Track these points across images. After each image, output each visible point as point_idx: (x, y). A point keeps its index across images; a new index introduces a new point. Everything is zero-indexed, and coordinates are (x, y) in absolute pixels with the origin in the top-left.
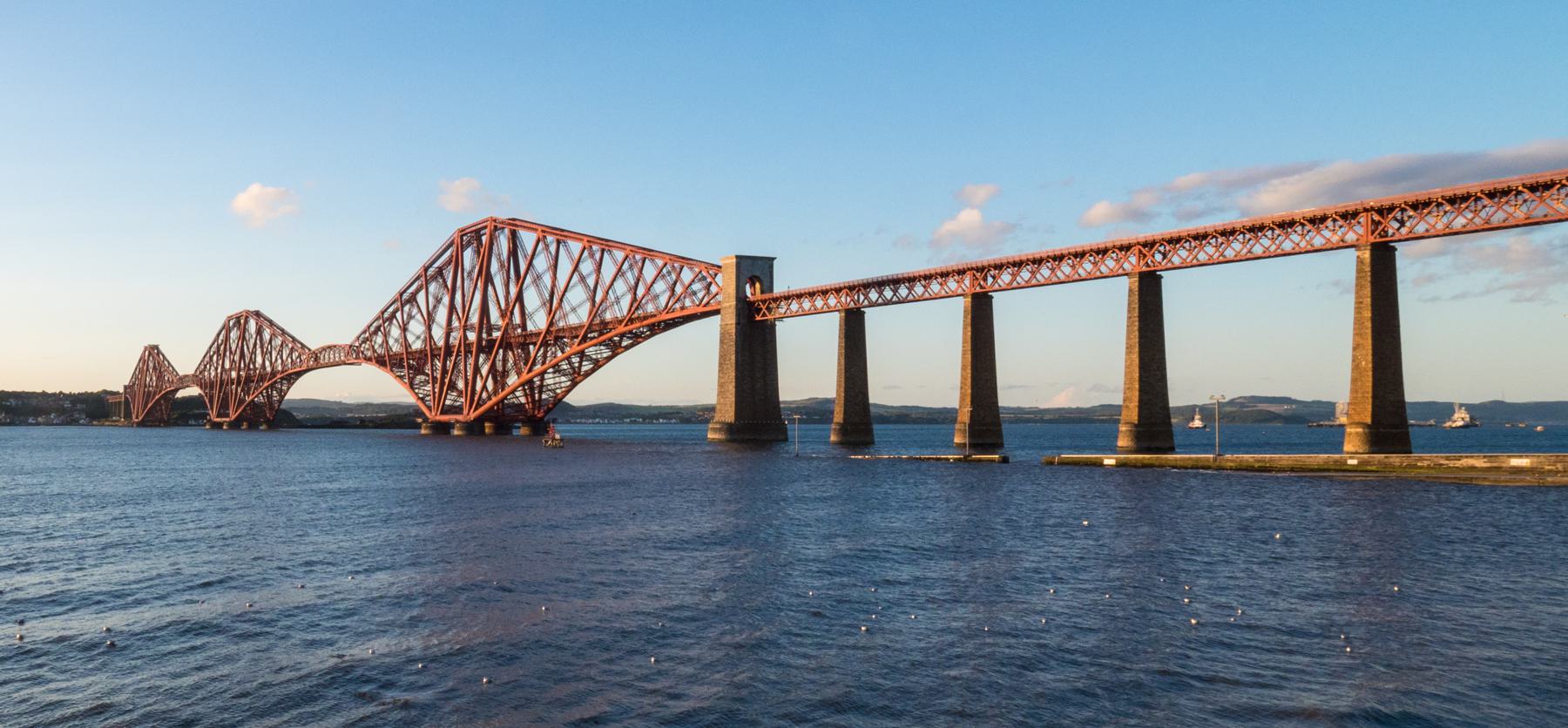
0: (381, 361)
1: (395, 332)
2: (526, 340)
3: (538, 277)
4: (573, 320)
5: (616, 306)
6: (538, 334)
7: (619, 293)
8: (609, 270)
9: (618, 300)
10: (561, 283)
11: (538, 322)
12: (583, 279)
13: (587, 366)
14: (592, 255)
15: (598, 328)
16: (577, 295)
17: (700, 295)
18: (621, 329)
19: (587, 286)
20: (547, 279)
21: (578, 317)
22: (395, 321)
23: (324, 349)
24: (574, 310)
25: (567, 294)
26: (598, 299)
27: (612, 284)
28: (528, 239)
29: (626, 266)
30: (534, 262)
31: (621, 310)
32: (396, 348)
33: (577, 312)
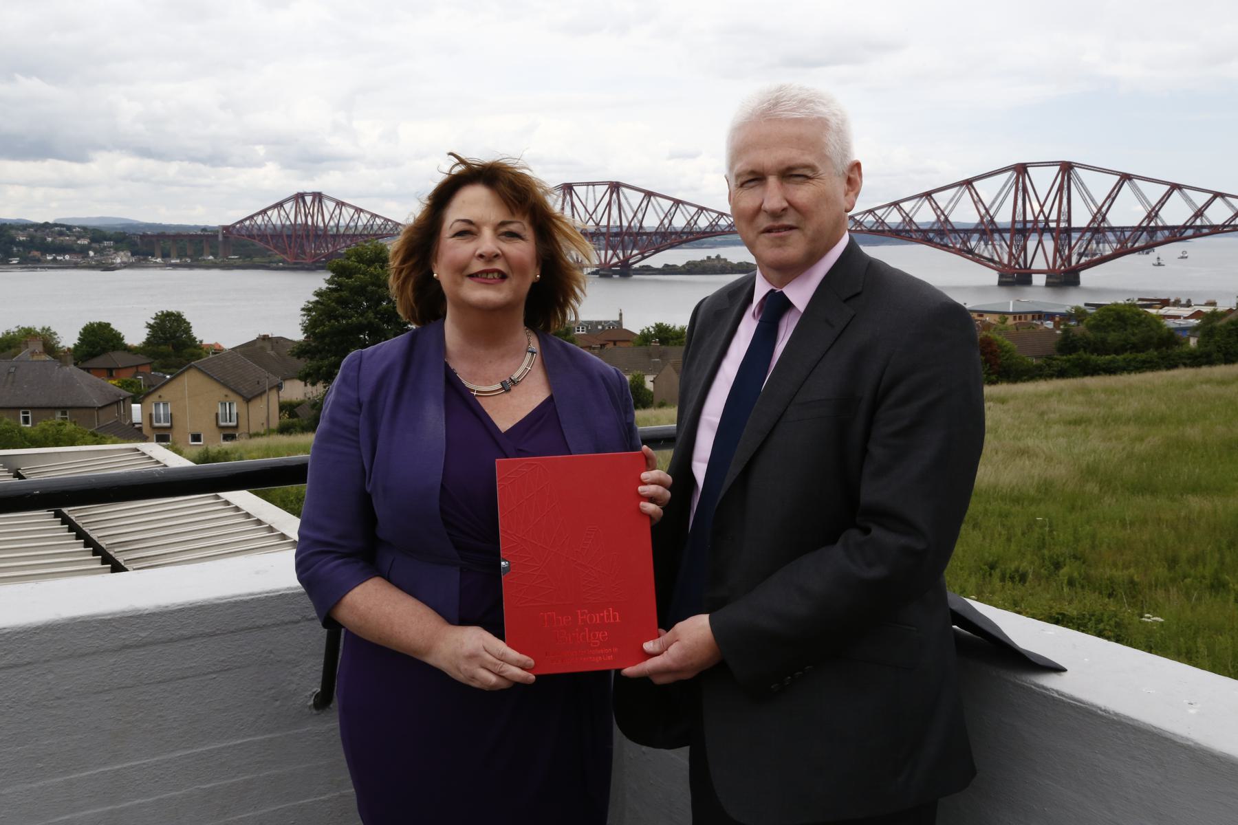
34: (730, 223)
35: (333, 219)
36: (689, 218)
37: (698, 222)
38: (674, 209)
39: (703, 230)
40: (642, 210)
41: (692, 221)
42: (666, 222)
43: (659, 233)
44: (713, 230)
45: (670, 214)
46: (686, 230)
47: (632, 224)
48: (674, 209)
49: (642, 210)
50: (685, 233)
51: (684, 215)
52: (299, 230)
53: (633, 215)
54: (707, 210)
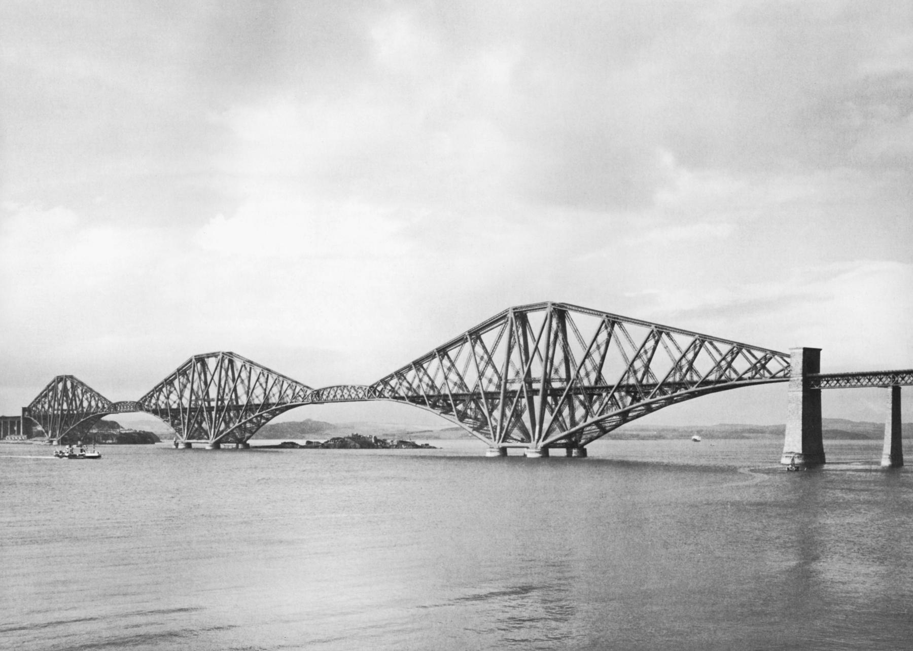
0: (155, 412)
1: (162, 398)
2: (238, 408)
3: (242, 381)
4: (256, 402)
5: (273, 398)
6: (243, 406)
7: (274, 393)
8: (271, 382)
9: (274, 395)
10: (252, 386)
11: (243, 400)
12: (261, 385)
13: (263, 421)
14: (263, 375)
15: (266, 405)
16: (259, 391)
17: (302, 396)
18: (274, 407)
19: (262, 387)
20: (246, 382)
21: (259, 400)
22: (162, 393)
23: (120, 403)
24: (257, 397)
25: (254, 391)
26: (267, 393)
27: (271, 389)
28: (238, 364)
29: (277, 382)
30: (242, 375)
31: (275, 399)
32: (163, 407)
33: (258, 399)
34: (754, 361)
35: (594, 368)
36: (678, 356)
37: (695, 364)
38: (651, 343)
39: (703, 375)
40: (598, 347)
41: (684, 362)
42: (638, 364)
43: (624, 386)
44: (723, 378)
45: (646, 352)
46: (670, 380)
47: (582, 372)
48: (651, 343)
49: (598, 347)
50: (669, 385)
51: (669, 352)
52: (513, 382)
53: (583, 354)
54: (712, 340)
